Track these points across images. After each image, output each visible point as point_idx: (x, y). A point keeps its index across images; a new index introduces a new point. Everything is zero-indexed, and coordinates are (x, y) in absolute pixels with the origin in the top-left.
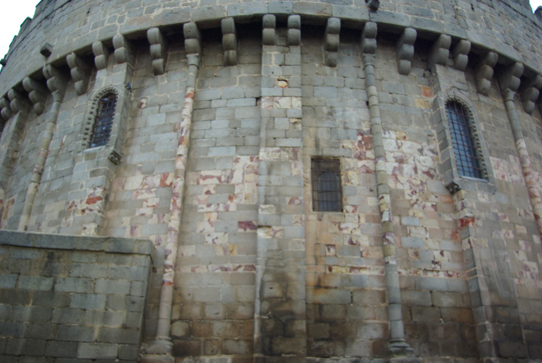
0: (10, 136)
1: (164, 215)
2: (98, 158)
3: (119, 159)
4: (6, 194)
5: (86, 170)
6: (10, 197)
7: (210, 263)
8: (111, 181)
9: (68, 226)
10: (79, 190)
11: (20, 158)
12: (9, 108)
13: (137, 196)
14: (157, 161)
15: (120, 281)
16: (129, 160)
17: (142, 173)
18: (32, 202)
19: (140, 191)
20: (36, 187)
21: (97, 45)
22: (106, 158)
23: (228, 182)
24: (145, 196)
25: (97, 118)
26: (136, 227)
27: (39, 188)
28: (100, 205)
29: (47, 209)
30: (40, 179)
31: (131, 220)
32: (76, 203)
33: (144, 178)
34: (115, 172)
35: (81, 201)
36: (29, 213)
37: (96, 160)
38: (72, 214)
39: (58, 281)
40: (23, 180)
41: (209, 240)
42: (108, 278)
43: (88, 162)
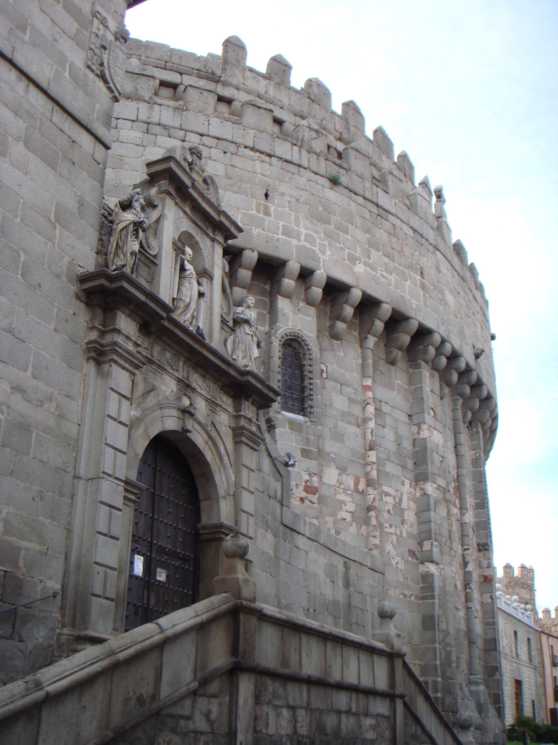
1: (361, 526)
7: (396, 587)
13: (336, 494)
17: (337, 468)
21: (294, 266)
23: (400, 505)
24: (341, 497)
41: (394, 562)
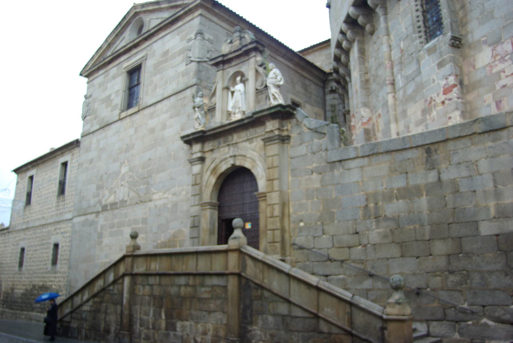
0: (357, 63)
2: (440, 49)
3: (460, 42)
4: (371, 111)
5: (432, 65)
6: (376, 112)
8: (460, 65)
9: (433, 120)
10: (432, 85)
11: (372, 78)
12: (347, 40)
13: (491, 70)
14: (501, 27)
15: (501, 157)
16: (470, 38)
17: (489, 46)
18: (395, 110)
19: (493, 64)
20: (394, 97)
22: (447, 46)
24: (500, 66)
25: (424, 12)
26: (500, 101)
27: (396, 97)
28: (457, 92)
29: (410, 112)
30: (394, 88)
31: (494, 96)
32: (434, 98)
33: (492, 50)
34: (461, 56)
35: (438, 95)
36: (396, 121)
37: (438, 51)
38: (433, 109)
39: (441, 171)
40: (381, 94)
42: (488, 157)
43: (431, 56)
